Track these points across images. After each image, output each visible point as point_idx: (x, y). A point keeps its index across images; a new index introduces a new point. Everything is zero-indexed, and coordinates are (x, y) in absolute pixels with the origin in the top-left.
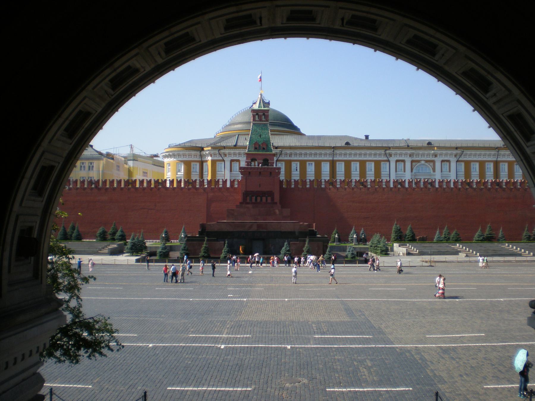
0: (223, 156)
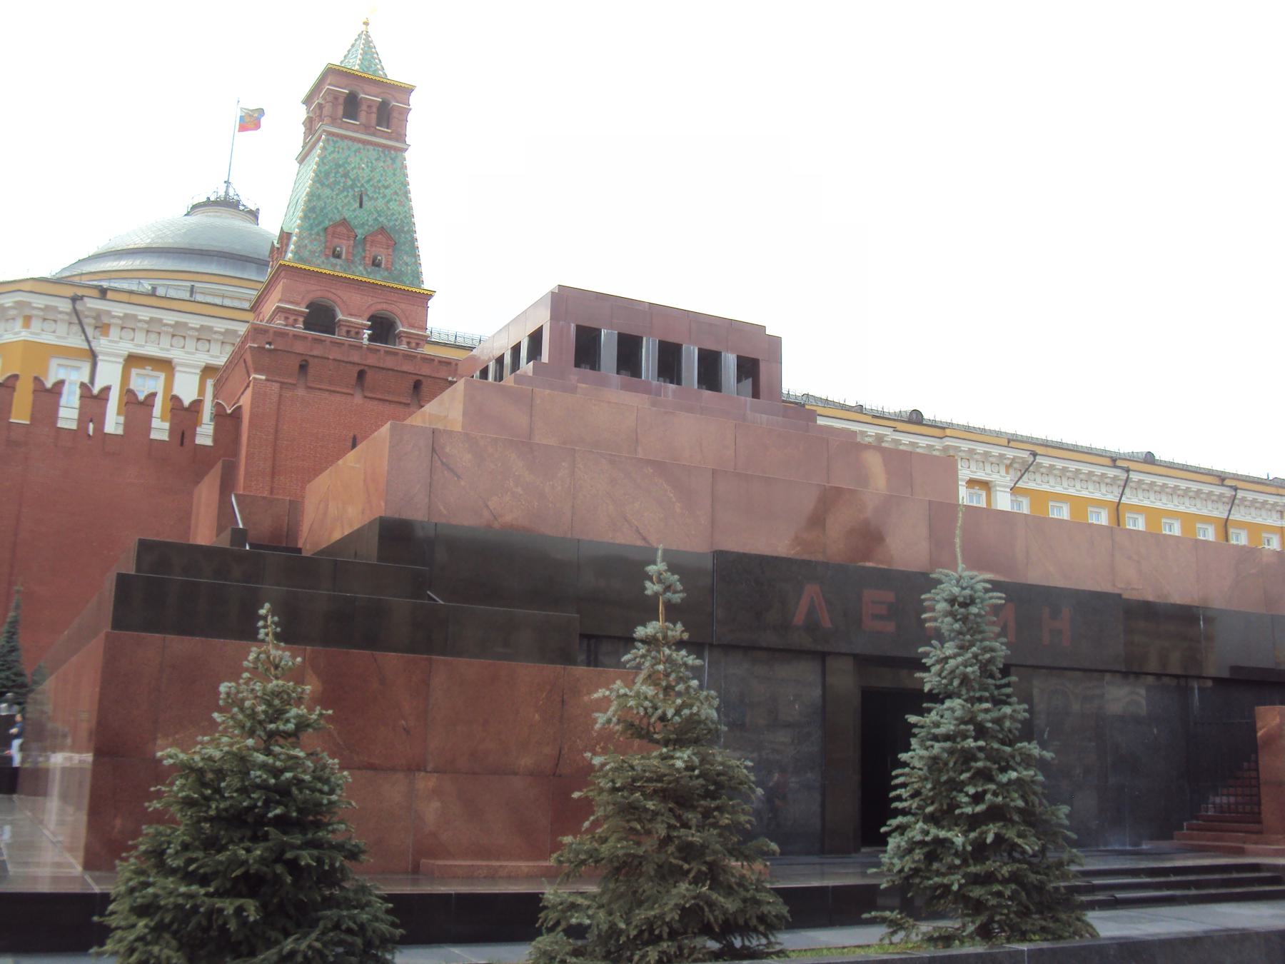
0: (90, 331)
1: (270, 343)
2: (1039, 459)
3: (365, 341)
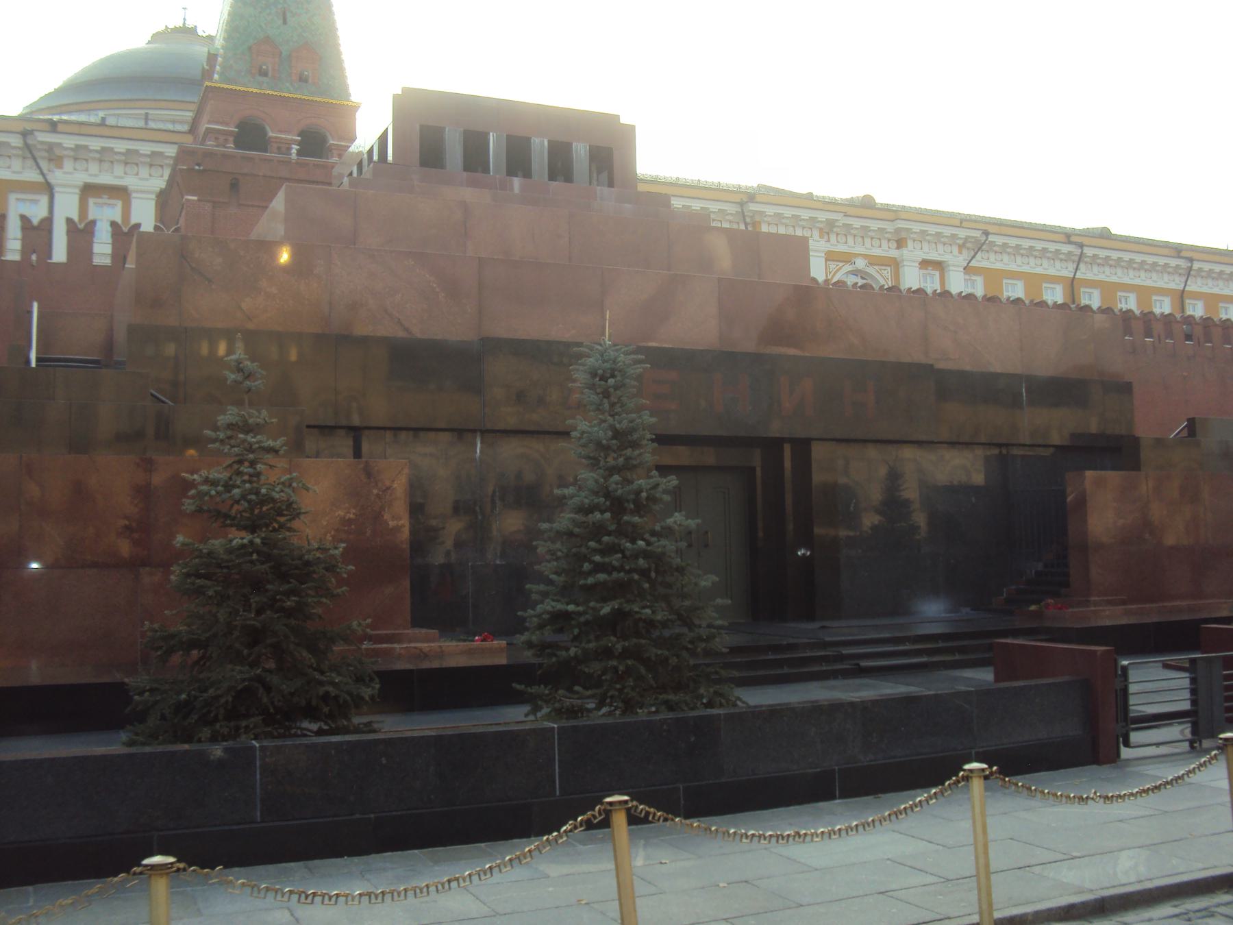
0: (44, 165)
1: (198, 165)
2: (991, 238)
3: (294, 156)
